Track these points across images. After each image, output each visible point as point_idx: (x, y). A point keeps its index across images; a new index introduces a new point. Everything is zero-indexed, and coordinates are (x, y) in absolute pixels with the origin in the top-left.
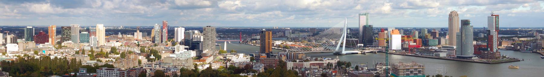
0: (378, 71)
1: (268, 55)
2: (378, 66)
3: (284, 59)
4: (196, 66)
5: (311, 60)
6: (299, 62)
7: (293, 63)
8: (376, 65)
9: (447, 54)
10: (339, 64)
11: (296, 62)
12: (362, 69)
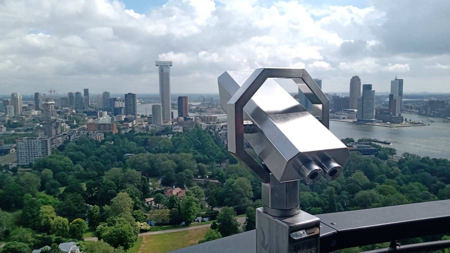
1: (186, 119)
7: (207, 125)
11: (210, 123)
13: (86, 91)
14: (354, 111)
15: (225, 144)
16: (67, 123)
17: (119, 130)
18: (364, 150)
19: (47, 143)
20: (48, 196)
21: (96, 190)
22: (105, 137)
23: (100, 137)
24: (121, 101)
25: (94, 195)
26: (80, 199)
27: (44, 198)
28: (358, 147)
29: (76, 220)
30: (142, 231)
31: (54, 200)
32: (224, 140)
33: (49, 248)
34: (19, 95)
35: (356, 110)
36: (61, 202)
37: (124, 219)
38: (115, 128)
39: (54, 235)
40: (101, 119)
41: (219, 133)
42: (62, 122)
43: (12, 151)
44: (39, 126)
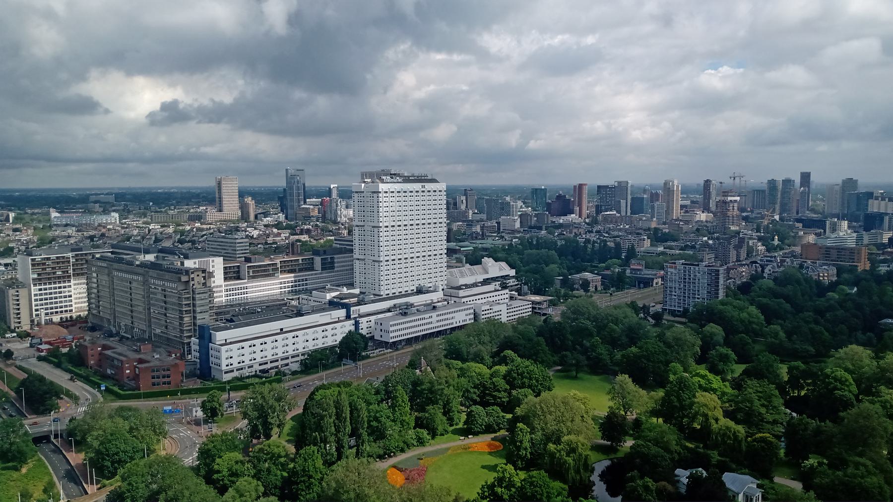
13: (806, 177)
16: (760, 239)
17: (874, 263)
19: (718, 275)
20: (711, 376)
21: (808, 385)
22: (838, 275)
23: (827, 274)
24: (883, 199)
25: (803, 393)
26: (772, 395)
27: (703, 377)
29: (761, 435)
31: (722, 387)
33: (705, 474)
34: (676, 183)
36: (736, 392)
37: (869, 463)
38: (863, 257)
39: (716, 452)
40: (833, 236)
42: (750, 239)
43: (657, 284)
44: (706, 242)
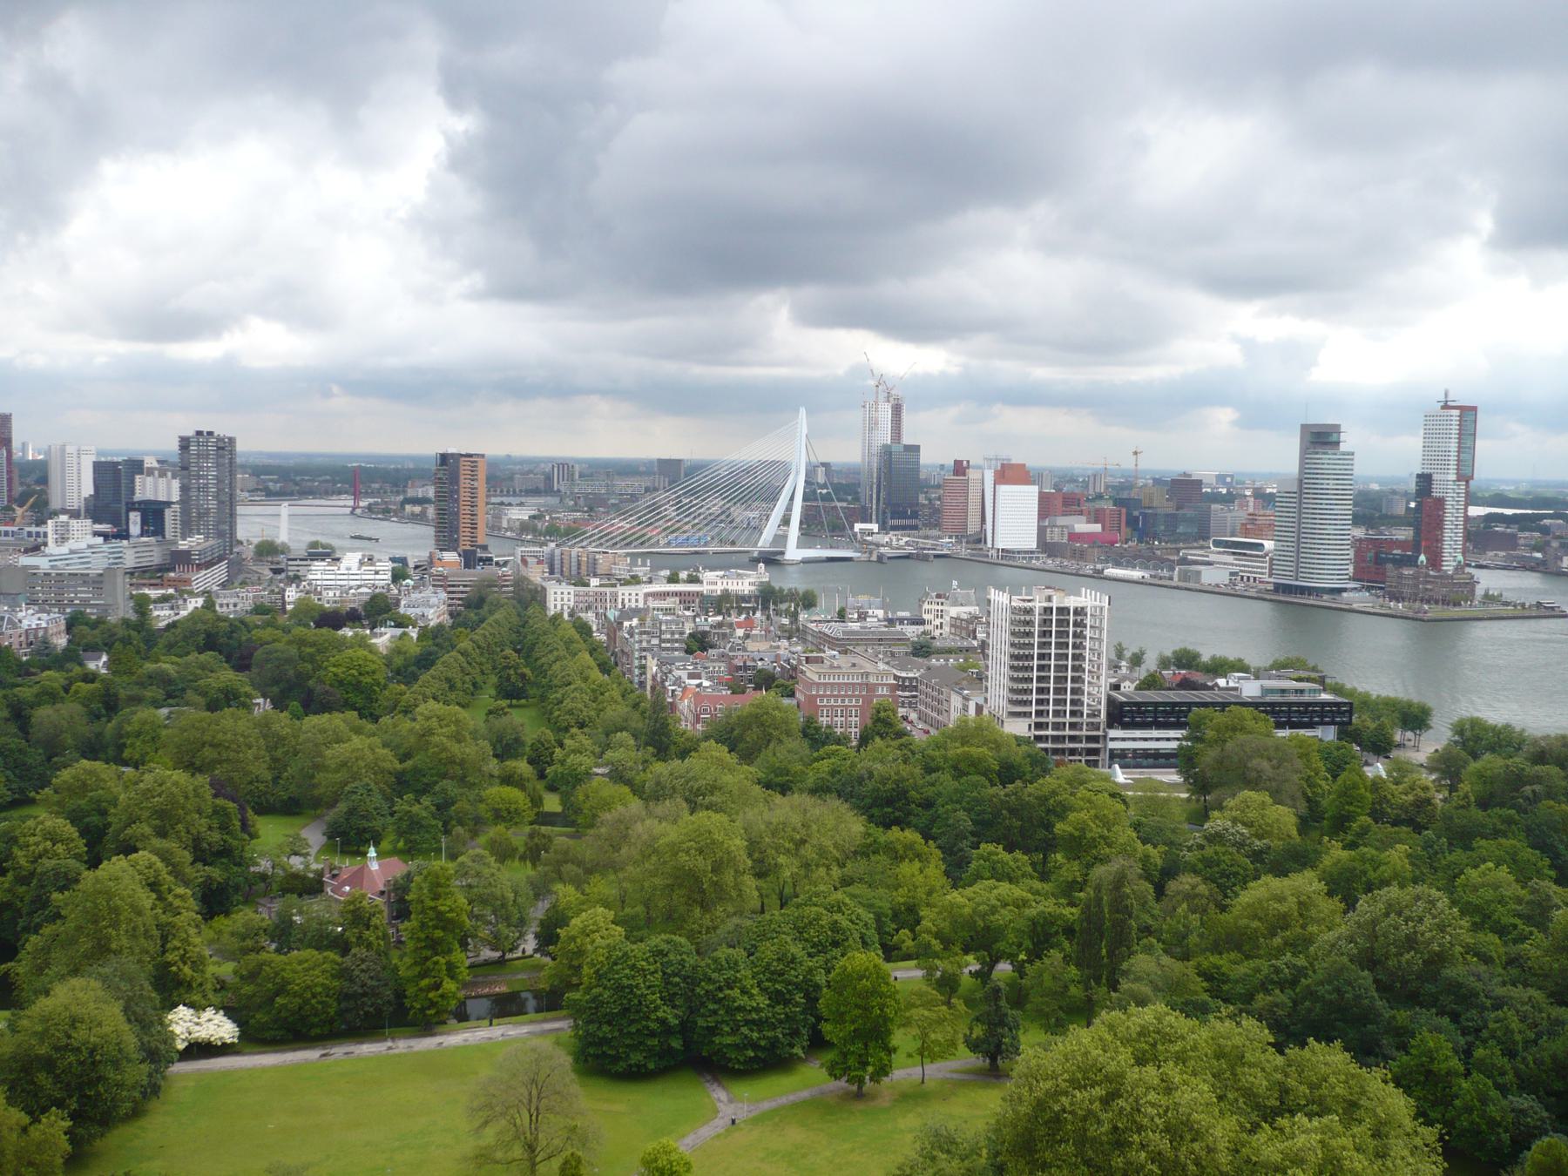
0: (928, 627)
1: (470, 560)
2: (930, 607)
3: (536, 574)
4: (142, 605)
5: (650, 581)
6: (601, 585)
7: (572, 589)
8: (921, 602)
9: (1232, 574)
10: (767, 597)
12: (862, 617)
14: (1262, 545)
15: (649, 676)
18: (1290, 704)
24: (163, 474)
28: (1266, 691)
30: (201, 1049)
32: (645, 658)
35: (1269, 545)
41: (626, 624)
